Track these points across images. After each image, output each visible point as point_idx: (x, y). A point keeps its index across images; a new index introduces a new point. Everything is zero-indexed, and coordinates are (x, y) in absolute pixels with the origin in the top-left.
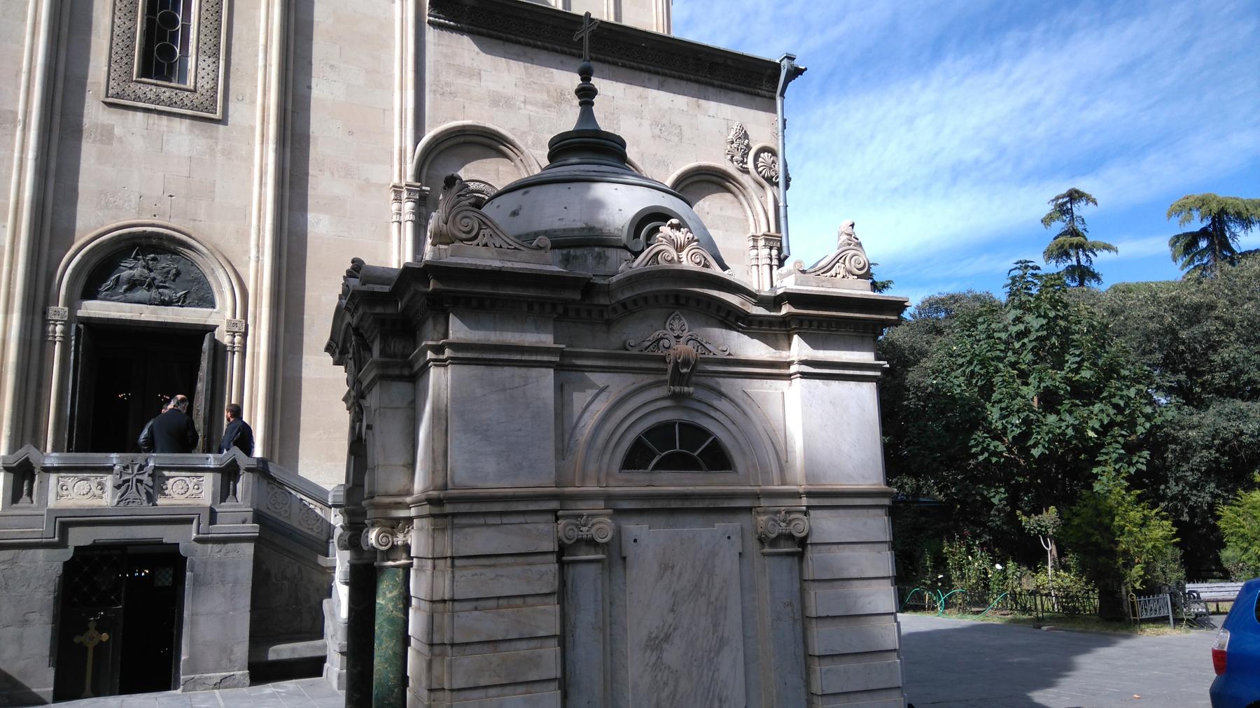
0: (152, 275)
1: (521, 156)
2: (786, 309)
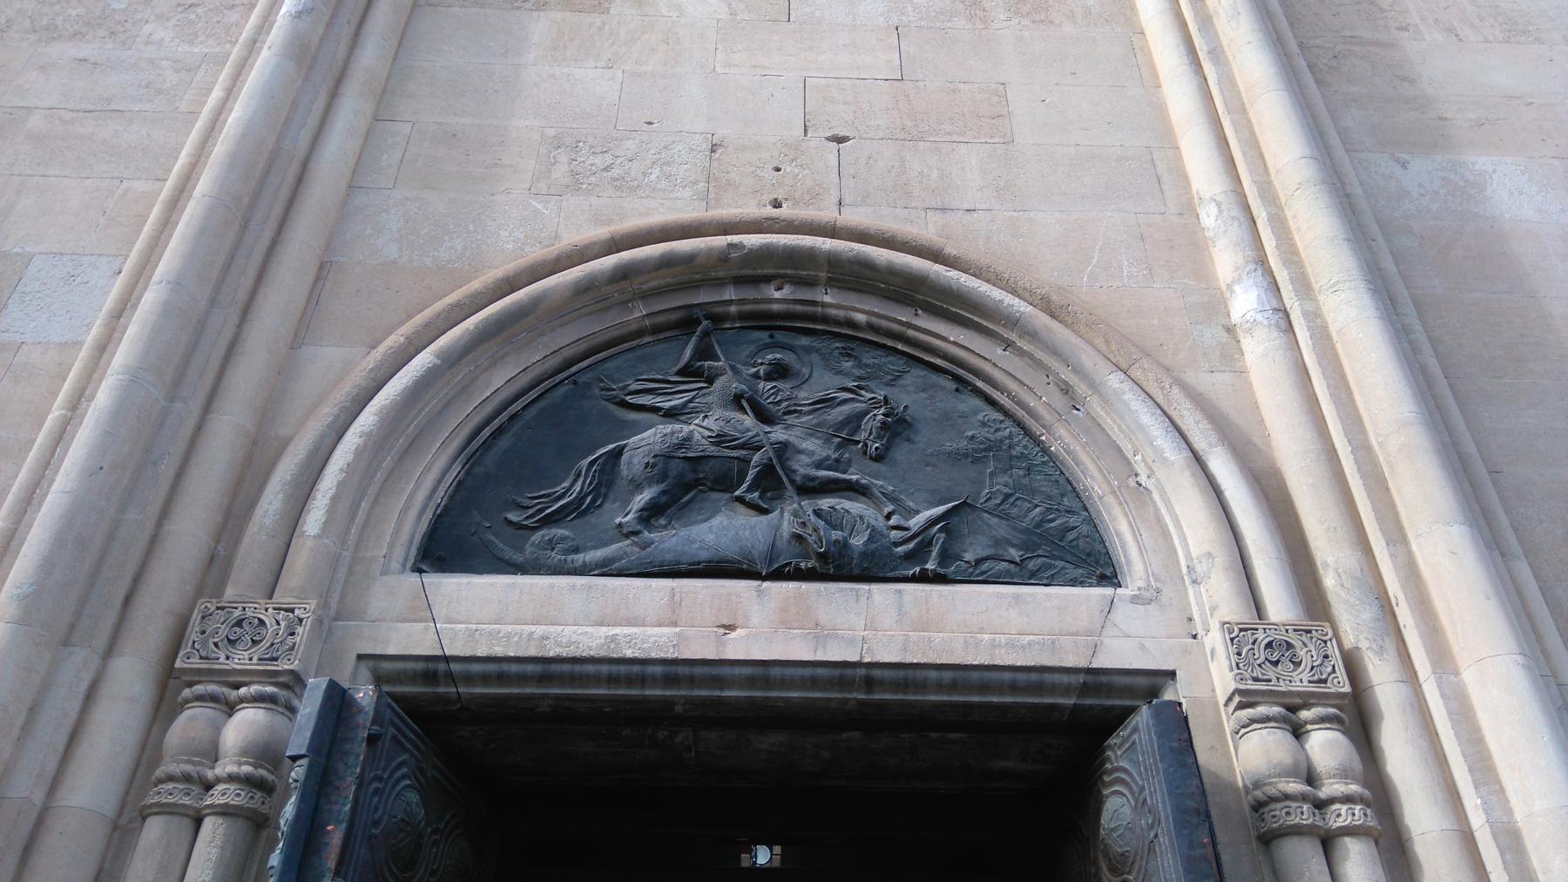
0: (778, 434)
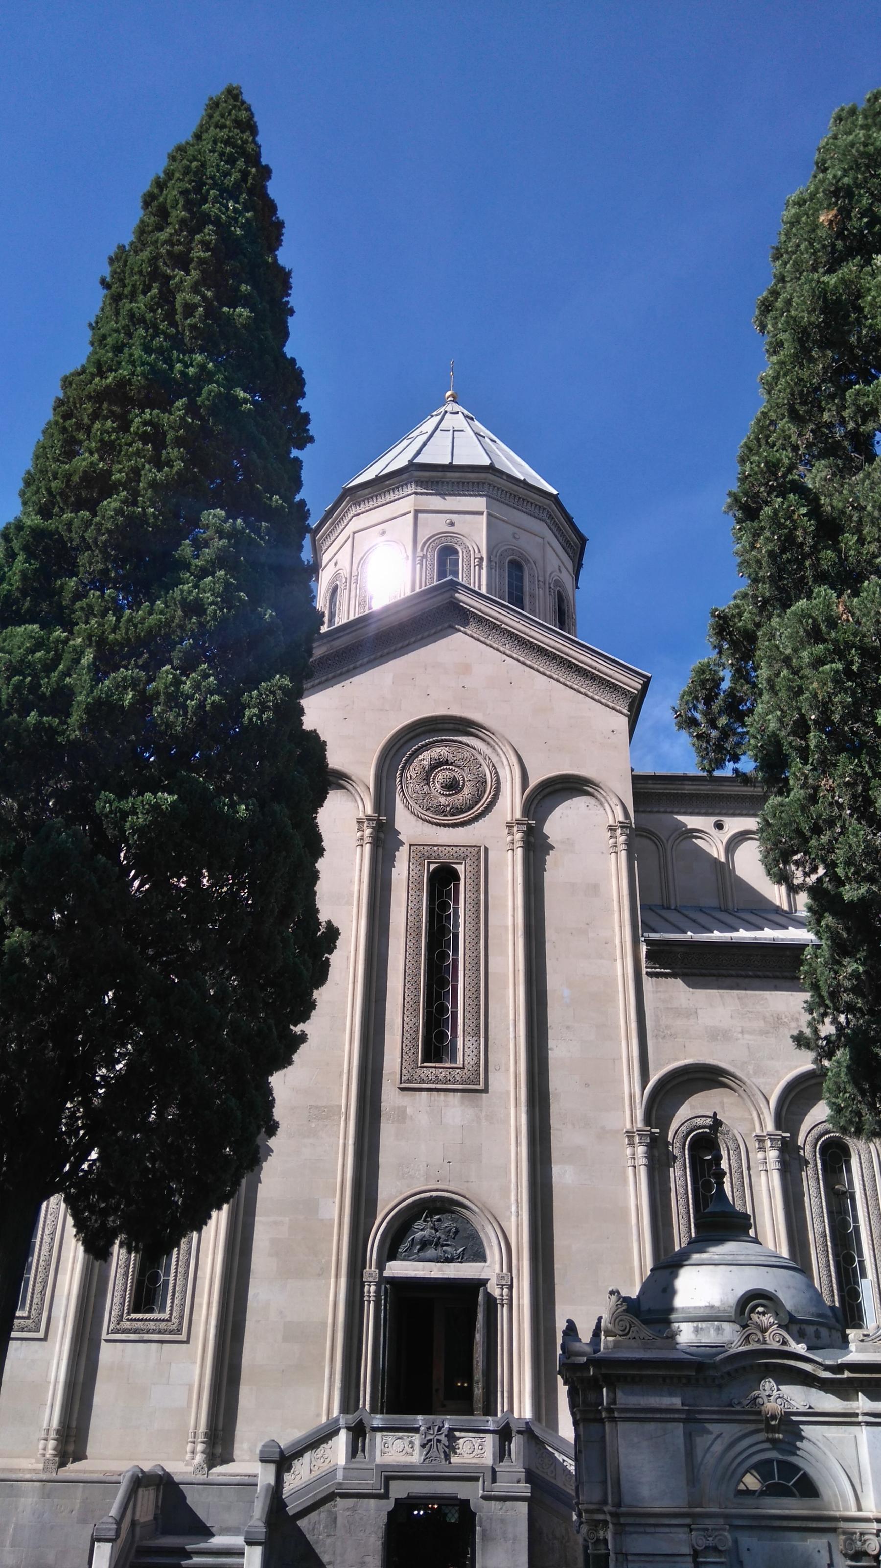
1: (744, 1087)
2: (847, 1374)
